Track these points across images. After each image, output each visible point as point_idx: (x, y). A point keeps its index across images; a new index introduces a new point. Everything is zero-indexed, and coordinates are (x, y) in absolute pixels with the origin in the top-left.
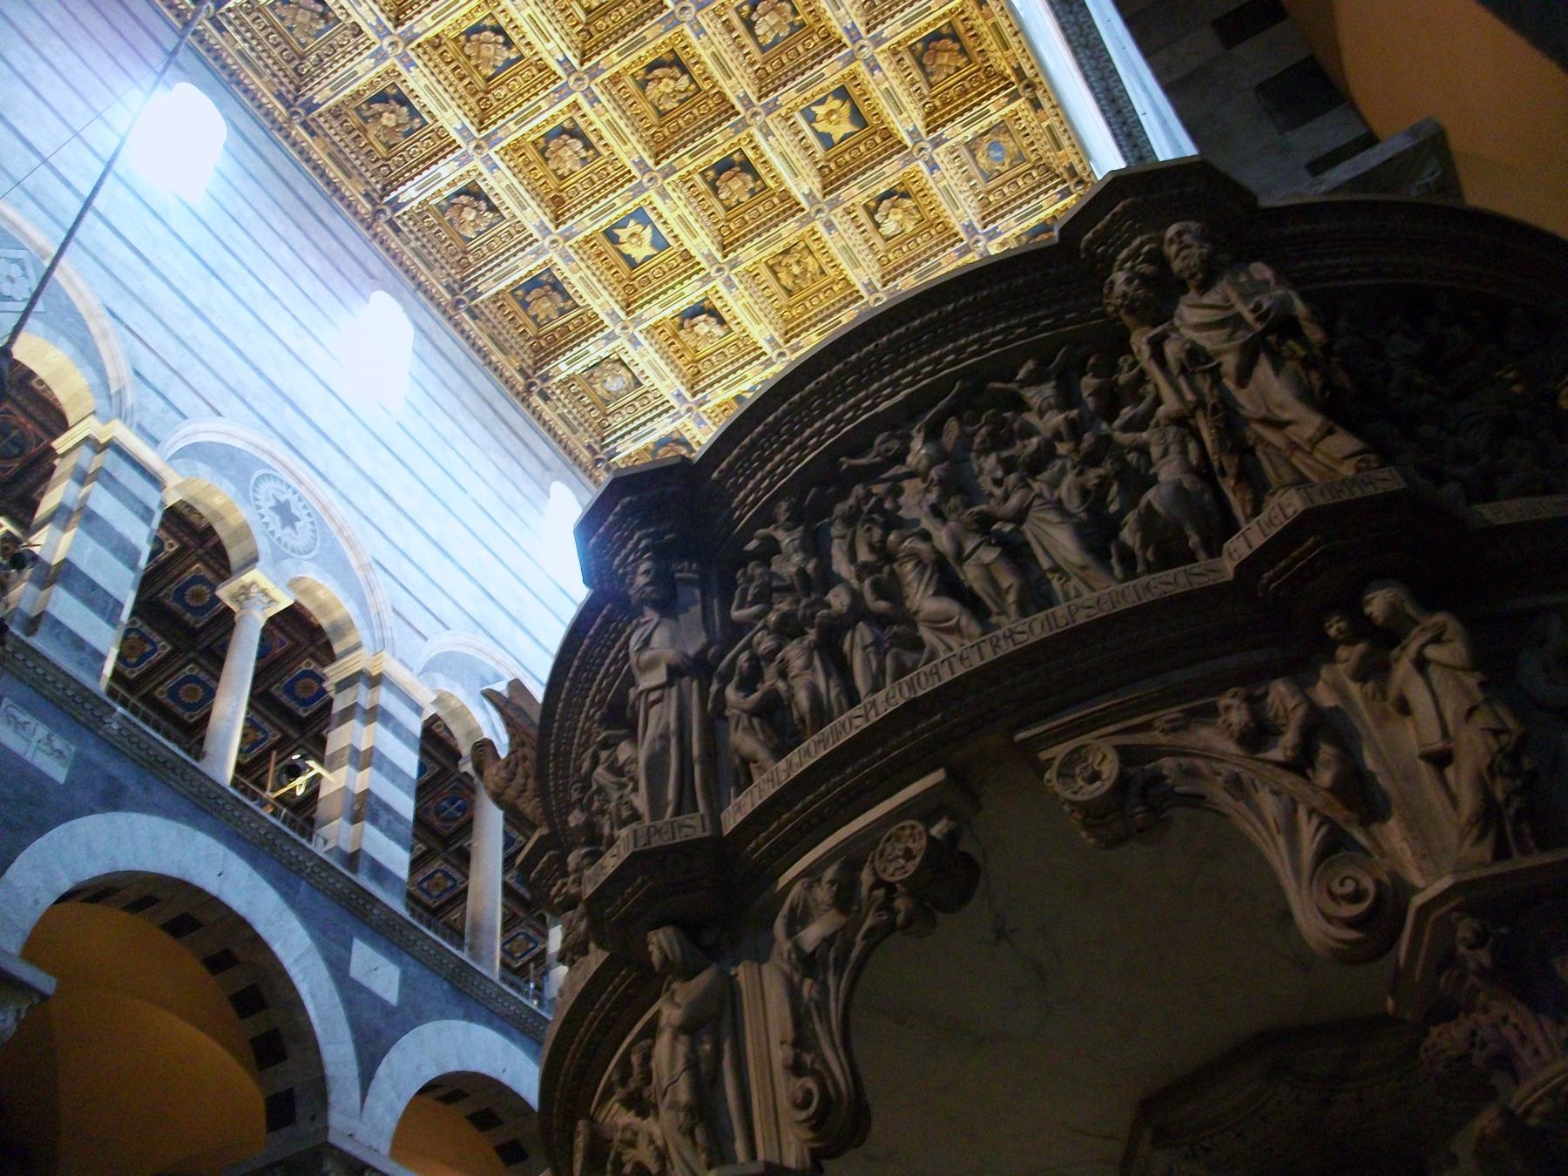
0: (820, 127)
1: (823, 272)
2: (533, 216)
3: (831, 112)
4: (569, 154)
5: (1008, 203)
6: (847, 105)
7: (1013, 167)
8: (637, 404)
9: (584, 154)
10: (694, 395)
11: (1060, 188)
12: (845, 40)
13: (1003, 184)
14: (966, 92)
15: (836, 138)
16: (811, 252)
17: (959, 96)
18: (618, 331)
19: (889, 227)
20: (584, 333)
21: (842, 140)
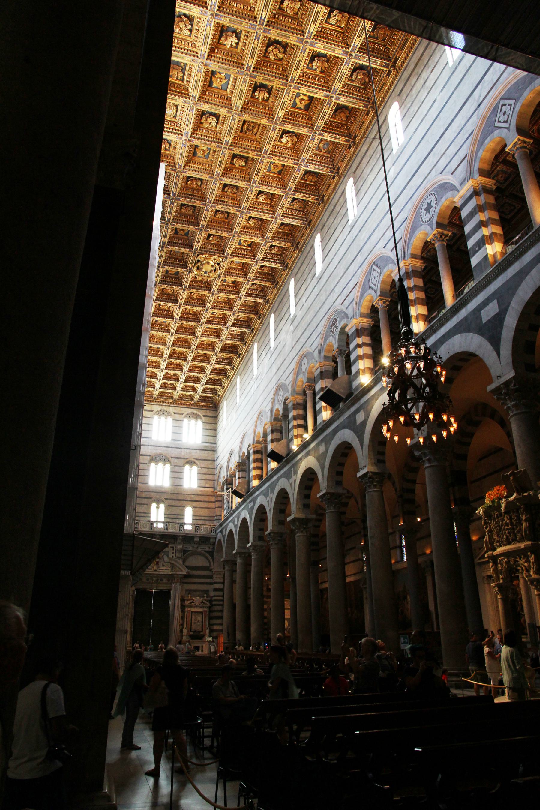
0: (297, 101)
1: (256, 134)
2: (204, 50)
3: (303, 100)
4: (230, 41)
5: (317, 161)
6: (309, 102)
7: (325, 152)
8: (170, 123)
9: (234, 44)
10: (190, 137)
11: (332, 170)
12: (331, 91)
13: (319, 155)
14: (338, 128)
15: (297, 107)
16: (259, 127)
17: (335, 127)
18: (191, 102)
19: (284, 140)
20: (179, 93)
21: (298, 108)
